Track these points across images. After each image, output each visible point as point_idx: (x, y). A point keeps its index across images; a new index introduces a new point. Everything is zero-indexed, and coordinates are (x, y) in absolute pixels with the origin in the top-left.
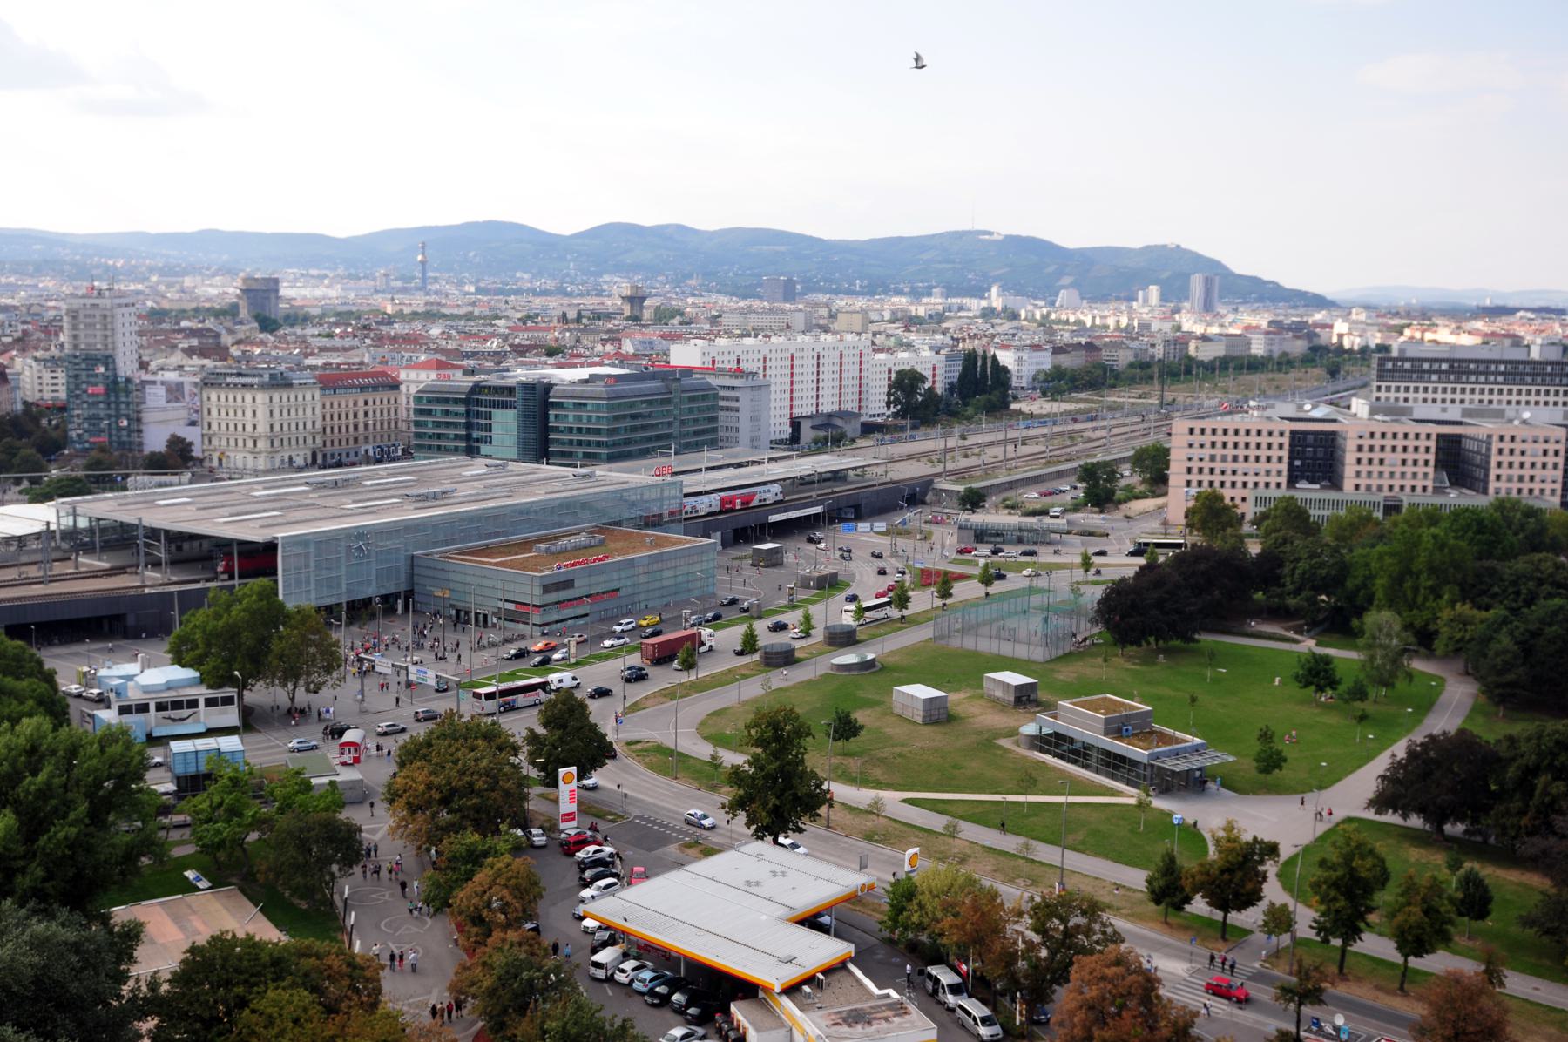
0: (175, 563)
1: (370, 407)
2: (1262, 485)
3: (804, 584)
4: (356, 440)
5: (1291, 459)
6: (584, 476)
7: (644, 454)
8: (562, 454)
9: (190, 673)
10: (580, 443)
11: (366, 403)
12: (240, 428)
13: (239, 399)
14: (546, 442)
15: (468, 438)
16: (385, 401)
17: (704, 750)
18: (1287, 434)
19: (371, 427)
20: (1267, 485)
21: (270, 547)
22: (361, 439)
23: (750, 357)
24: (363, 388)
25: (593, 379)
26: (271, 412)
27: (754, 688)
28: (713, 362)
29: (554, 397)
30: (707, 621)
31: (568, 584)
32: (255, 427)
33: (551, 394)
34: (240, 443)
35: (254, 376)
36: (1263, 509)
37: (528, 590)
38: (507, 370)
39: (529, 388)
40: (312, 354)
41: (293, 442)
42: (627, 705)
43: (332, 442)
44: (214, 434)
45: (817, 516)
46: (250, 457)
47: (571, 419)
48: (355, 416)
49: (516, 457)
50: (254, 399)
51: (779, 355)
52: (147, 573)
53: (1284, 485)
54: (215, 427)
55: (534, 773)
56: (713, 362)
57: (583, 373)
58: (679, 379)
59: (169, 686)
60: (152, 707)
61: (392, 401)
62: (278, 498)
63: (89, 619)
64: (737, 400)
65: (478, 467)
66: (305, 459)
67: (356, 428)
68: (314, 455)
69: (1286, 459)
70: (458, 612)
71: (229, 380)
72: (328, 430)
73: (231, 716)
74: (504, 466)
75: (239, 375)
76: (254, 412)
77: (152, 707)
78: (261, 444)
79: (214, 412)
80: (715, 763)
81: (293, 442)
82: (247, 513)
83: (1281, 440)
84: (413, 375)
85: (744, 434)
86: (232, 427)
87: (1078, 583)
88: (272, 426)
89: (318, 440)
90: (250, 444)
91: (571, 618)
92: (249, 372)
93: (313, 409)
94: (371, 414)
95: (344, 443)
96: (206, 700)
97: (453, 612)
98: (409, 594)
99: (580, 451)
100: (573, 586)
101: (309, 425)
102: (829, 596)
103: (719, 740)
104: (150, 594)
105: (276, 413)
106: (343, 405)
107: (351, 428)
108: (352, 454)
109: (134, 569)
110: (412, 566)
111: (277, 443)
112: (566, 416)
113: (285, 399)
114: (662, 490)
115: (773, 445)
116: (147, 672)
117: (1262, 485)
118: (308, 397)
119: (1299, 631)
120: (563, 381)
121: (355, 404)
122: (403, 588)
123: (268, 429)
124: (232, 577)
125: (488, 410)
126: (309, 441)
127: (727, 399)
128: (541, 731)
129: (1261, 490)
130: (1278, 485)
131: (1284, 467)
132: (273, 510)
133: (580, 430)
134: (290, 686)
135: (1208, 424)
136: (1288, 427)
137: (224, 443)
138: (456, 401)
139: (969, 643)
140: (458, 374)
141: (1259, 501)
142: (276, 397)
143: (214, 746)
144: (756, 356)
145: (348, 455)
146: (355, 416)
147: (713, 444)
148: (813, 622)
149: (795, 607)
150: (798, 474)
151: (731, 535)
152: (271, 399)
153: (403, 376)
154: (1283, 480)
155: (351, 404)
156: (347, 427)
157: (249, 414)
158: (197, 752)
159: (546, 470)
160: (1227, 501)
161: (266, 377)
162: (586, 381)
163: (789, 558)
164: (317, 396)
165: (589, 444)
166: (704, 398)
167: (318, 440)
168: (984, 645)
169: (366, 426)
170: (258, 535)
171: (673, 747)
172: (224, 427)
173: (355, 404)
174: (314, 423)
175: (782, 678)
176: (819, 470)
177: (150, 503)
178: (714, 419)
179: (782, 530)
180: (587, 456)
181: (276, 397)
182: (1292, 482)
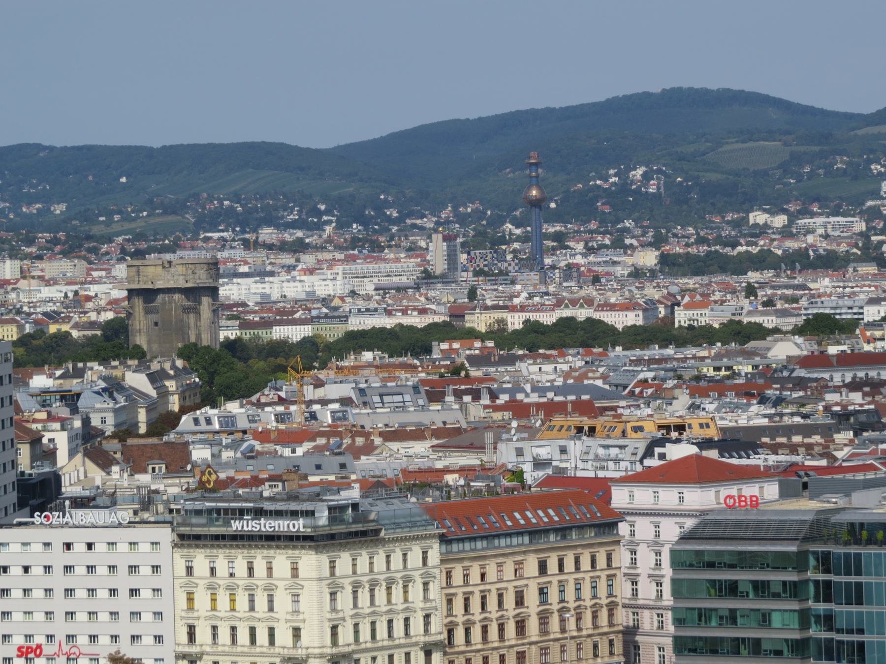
11: (543, 568)
12: (262, 637)
24: (536, 533)
32: (297, 633)
35: (294, 514)
40: (369, 449)
48: (520, 601)
67: (521, 627)
71: (236, 526)
75: (259, 513)
86: (243, 637)
107: (511, 629)
123: (328, 641)
138: (781, 562)
140: (771, 490)
142: (344, 560)
146: (520, 601)
161: (323, 517)
164: (434, 557)
172: (224, 636)
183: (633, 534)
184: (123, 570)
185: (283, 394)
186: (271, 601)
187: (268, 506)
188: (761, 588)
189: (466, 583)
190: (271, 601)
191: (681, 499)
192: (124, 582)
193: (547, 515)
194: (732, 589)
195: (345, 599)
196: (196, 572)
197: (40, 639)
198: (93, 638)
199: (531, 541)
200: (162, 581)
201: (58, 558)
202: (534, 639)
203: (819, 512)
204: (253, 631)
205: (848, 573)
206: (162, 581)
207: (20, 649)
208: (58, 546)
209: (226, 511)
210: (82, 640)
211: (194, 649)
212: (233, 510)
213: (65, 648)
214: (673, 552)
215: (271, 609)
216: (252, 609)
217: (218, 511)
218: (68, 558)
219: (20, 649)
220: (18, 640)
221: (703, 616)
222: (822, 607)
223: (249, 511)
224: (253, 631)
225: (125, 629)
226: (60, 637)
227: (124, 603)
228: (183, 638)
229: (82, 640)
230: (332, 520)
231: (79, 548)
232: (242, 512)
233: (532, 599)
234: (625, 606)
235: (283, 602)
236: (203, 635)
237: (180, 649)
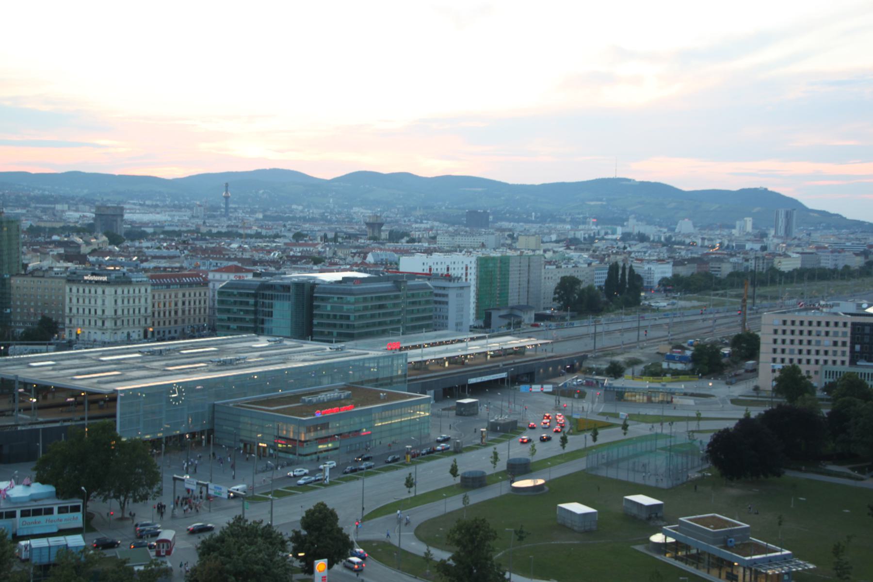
1: (187, 298)
2: (830, 362)
3: (493, 428)
4: (176, 322)
5: (853, 344)
8: (322, 333)
9: (49, 489)
10: (334, 325)
11: (184, 295)
12: (93, 312)
13: (93, 291)
14: (311, 325)
15: (255, 321)
16: (197, 294)
17: (418, 548)
18: (849, 325)
19: (187, 312)
20: (834, 362)
21: (113, 398)
22: (180, 321)
23: (456, 266)
24: (182, 285)
25: (345, 280)
26: (116, 301)
27: (454, 503)
28: (430, 270)
29: (317, 293)
30: (423, 455)
31: (325, 426)
32: (103, 311)
33: (315, 290)
34: (93, 323)
36: (831, 380)
38: (285, 274)
39: (300, 286)
40: (146, 260)
41: (131, 322)
42: (366, 513)
43: (159, 323)
44: (74, 316)
45: (502, 380)
46: (99, 333)
47: (329, 308)
48: (176, 305)
49: (289, 335)
50: (104, 292)
52: (20, 415)
53: (847, 363)
54: (74, 311)
55: (297, 564)
56: (430, 270)
57: (337, 276)
58: (406, 282)
59: (33, 499)
60: (18, 513)
61: (203, 294)
62: (118, 362)
65: (263, 342)
66: (139, 335)
67: (176, 312)
68: (146, 332)
69: (848, 344)
70: (245, 445)
72: (156, 314)
73: (76, 519)
74: (281, 341)
76: (103, 301)
77: (18, 513)
78: (109, 324)
79: (74, 300)
80: (427, 558)
81: (131, 322)
82: (96, 372)
83: (844, 329)
84: (218, 276)
85: (451, 321)
87: (693, 432)
88: (116, 311)
89: (149, 321)
90: (100, 323)
92: (101, 272)
93: (146, 299)
94: (187, 303)
97: (242, 445)
98: (211, 432)
99: (335, 331)
100: (328, 428)
101: (143, 311)
102: (512, 437)
103: (429, 541)
104: (22, 431)
105: (119, 302)
106: (168, 297)
107: (173, 313)
108: (173, 332)
109: (10, 413)
110: (213, 412)
111: (119, 323)
112: (326, 307)
113: (126, 291)
115: (473, 329)
117: (830, 362)
118: (143, 290)
119: (861, 470)
120: (324, 281)
121: (176, 296)
122: (207, 427)
123: (113, 313)
125: (270, 301)
126: (143, 322)
128: (304, 532)
129: (830, 367)
130: (843, 362)
131: (847, 349)
132: (115, 370)
133: (335, 316)
134: (122, 498)
135: (789, 318)
136: (850, 320)
138: (248, 295)
139: (611, 473)
141: (828, 374)
142: (119, 290)
143: (64, 543)
144: (461, 266)
145: (170, 332)
146: (176, 305)
147: (429, 328)
148: (499, 457)
149: (486, 445)
152: (116, 292)
153: (211, 276)
154: (847, 359)
155: (173, 296)
156: (170, 313)
157: (99, 302)
158: (50, 547)
159: (309, 345)
160: (804, 373)
163: (483, 411)
165: (341, 326)
167: (149, 321)
168: (622, 476)
169: (183, 312)
171: (398, 545)
172: (81, 311)
173: (176, 296)
174: (146, 309)
175: (476, 497)
176: (505, 347)
177: (26, 363)
179: (477, 390)
180: (340, 335)
181: (119, 290)
182: (853, 362)
183: (214, 287)
186: (96, 301)
187: (96, 272)
189: (159, 299)
190: (96, 301)
199: (180, 287)
211: (72, 314)
215: (96, 303)
222: (261, 309)
235: (99, 302)
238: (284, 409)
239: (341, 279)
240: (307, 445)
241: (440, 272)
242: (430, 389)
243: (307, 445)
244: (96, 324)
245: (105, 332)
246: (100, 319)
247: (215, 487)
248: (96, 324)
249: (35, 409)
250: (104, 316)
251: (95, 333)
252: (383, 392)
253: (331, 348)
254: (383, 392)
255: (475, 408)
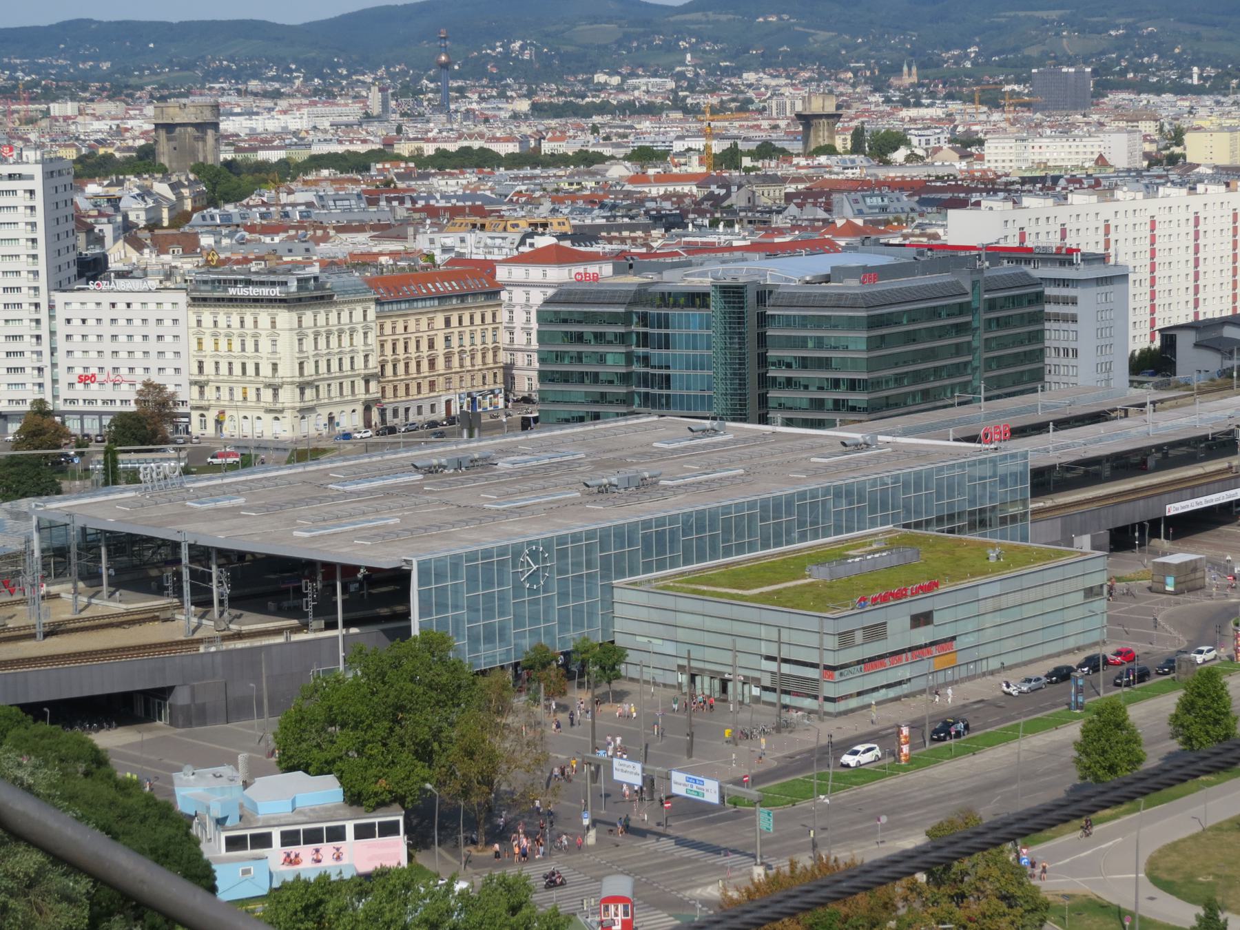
0: (243, 600)
4: (432, 385)
6: (858, 447)
7: (929, 399)
11: (448, 322)
12: (251, 370)
21: (400, 577)
23: (1082, 224)
24: (443, 298)
28: (1022, 236)
32: (275, 367)
34: (252, 395)
35: (273, 284)
37: (813, 640)
39: (733, 294)
40: (326, 238)
48: (431, 345)
50: (273, 323)
51: (1131, 220)
56: (1022, 236)
60: (276, 839)
63: (109, 698)
64: (1074, 301)
67: (432, 363)
71: (232, 292)
75: (248, 283)
77: (276, 839)
86: (237, 369)
91: (882, 687)
95: (413, 390)
96: (357, 827)
114: (995, 465)
116: (260, 782)
123: (297, 373)
124: (332, 625)
127: (1056, 300)
137: (225, 393)
138: (613, 319)
140: (607, 269)
142: (308, 316)
146: (431, 345)
150: (1210, 432)
151: (1106, 539)
161: (293, 286)
162: (827, 279)
164: (372, 314)
166: (1015, 301)
170: (385, 559)
172: (224, 369)
178: (1038, 336)
183: (510, 299)
184: (152, 322)
185: (265, 199)
186: (256, 345)
187: (254, 278)
188: (599, 337)
189: (394, 333)
190: (256, 345)
191: (545, 275)
192: (153, 330)
193: (451, 286)
194: (579, 338)
195: (308, 344)
196: (204, 324)
197: (94, 370)
198: (131, 369)
200: (179, 330)
201: (106, 313)
202: (442, 372)
203: (640, 285)
204: (244, 365)
205: (659, 327)
206: (179, 330)
207: (80, 377)
208: (106, 305)
209: (225, 281)
210: (124, 371)
211: (203, 378)
212: (230, 281)
213: (112, 377)
214: (538, 312)
215: (257, 350)
216: (243, 350)
217: (219, 281)
218: (113, 314)
219: (80, 377)
220: (79, 371)
221: (559, 356)
222: (641, 350)
223: (241, 281)
224: (244, 365)
225: (154, 363)
226: (108, 369)
227: (153, 345)
228: (196, 371)
229: (124, 371)
230: (300, 288)
231: (121, 306)
232: (236, 282)
233: (440, 344)
234: (505, 349)
235: (265, 345)
236: (209, 368)
237: (193, 378)
238: (769, 593)
239: (828, 271)
240: (841, 674)
241: (1043, 241)
242: (1082, 532)
243: (841, 674)
244: (258, 399)
245: (279, 416)
246: (268, 386)
247: (688, 780)
248: (258, 399)
249: (221, 602)
250: (277, 381)
251: (259, 418)
252: (993, 546)
253: (844, 444)
254: (993, 546)
255: (1199, 574)
